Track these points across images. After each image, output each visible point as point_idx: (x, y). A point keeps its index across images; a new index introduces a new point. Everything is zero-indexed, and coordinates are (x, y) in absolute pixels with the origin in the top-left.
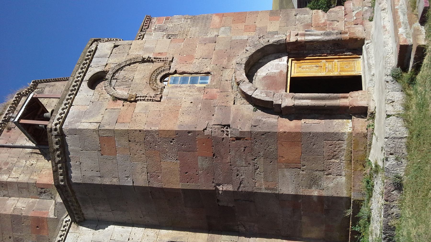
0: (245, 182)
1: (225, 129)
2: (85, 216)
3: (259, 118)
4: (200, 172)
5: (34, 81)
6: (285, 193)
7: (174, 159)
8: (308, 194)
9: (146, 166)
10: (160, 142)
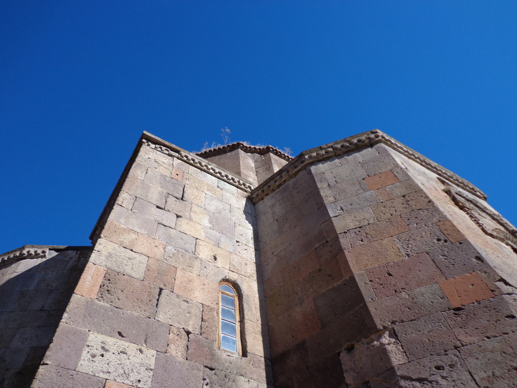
2: (261, 202)
4: (403, 294)
7: (407, 252)
9: (371, 221)
10: (428, 227)
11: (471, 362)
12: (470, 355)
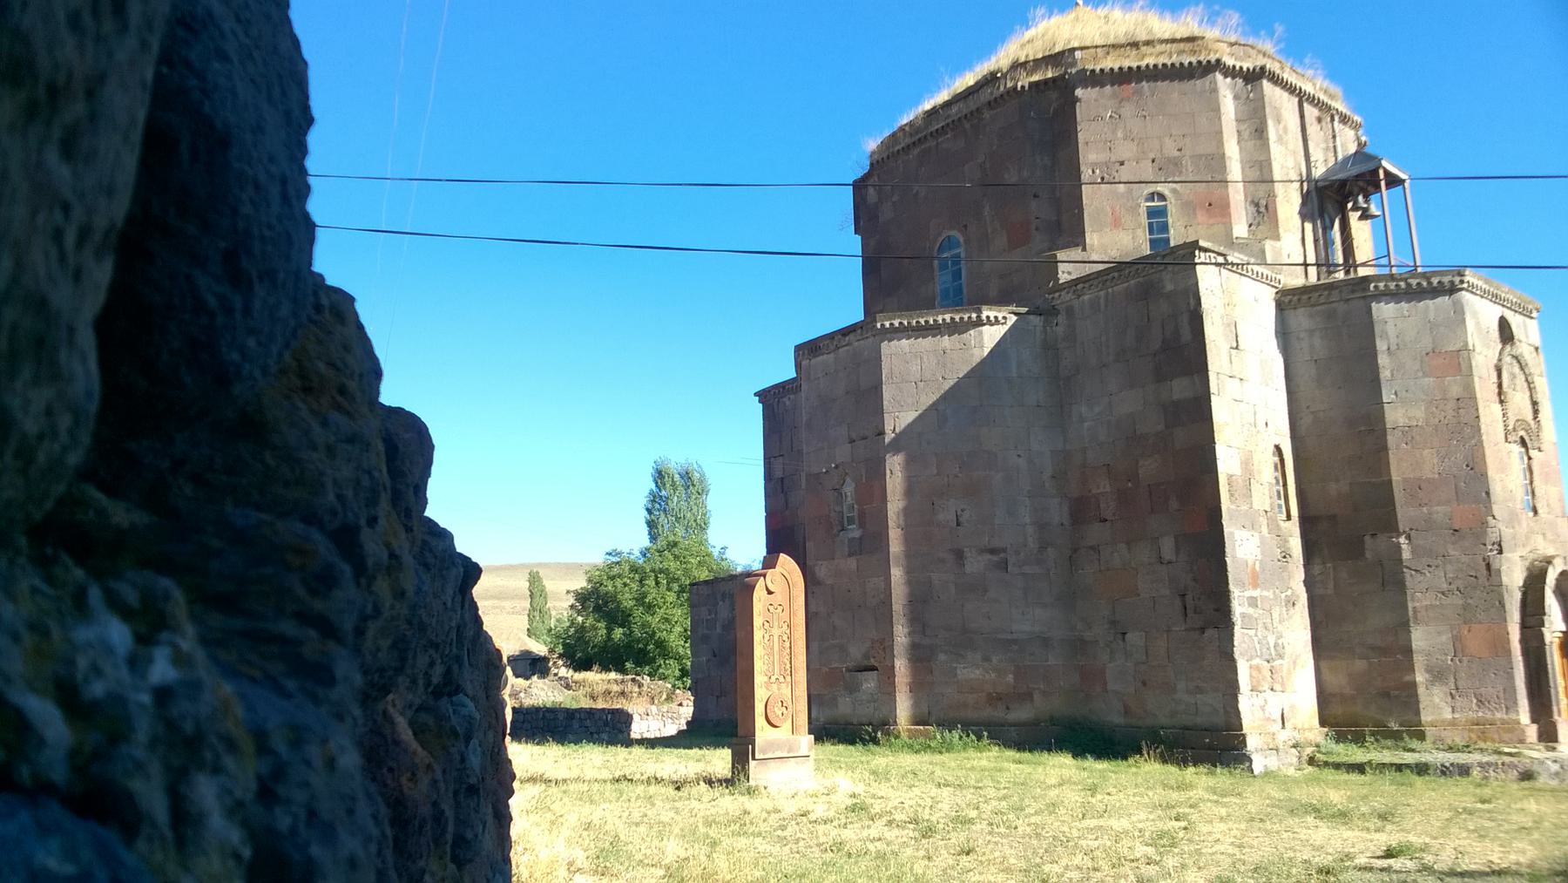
0: (1419, 577)
1: (1496, 547)
2: (1292, 311)
3: (1515, 598)
4: (1425, 509)
5: (1368, 143)
6: (1413, 636)
8: (1416, 668)
9: (1420, 424)
11: (1449, 567)
12: (1450, 562)
